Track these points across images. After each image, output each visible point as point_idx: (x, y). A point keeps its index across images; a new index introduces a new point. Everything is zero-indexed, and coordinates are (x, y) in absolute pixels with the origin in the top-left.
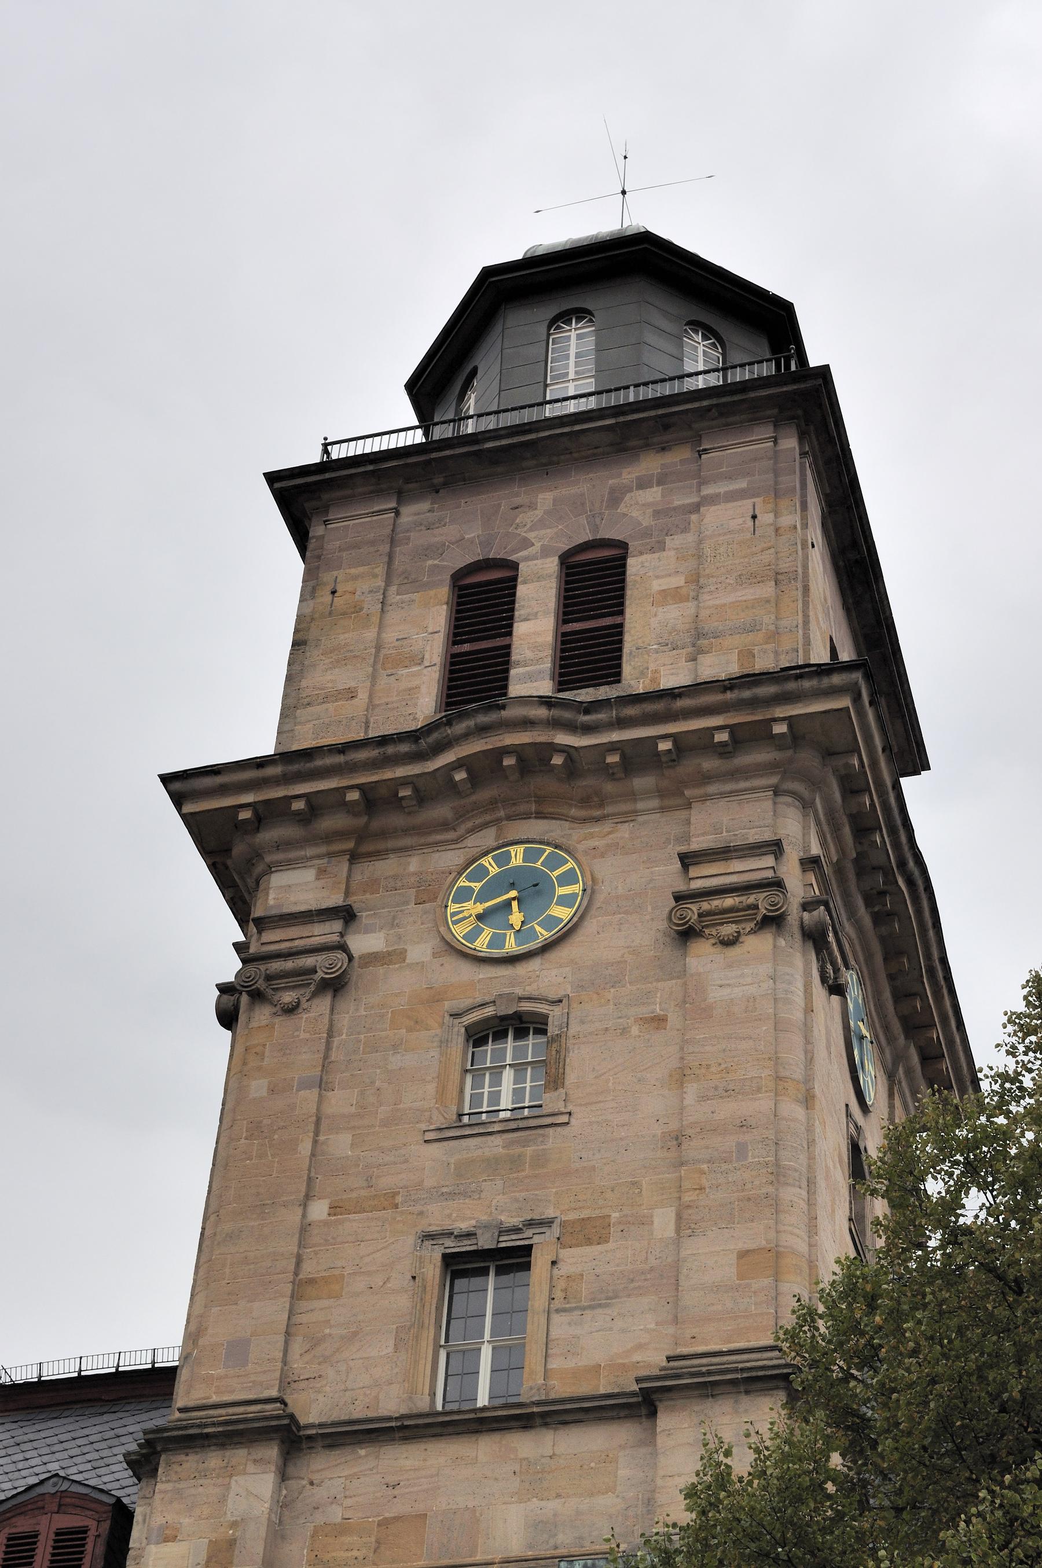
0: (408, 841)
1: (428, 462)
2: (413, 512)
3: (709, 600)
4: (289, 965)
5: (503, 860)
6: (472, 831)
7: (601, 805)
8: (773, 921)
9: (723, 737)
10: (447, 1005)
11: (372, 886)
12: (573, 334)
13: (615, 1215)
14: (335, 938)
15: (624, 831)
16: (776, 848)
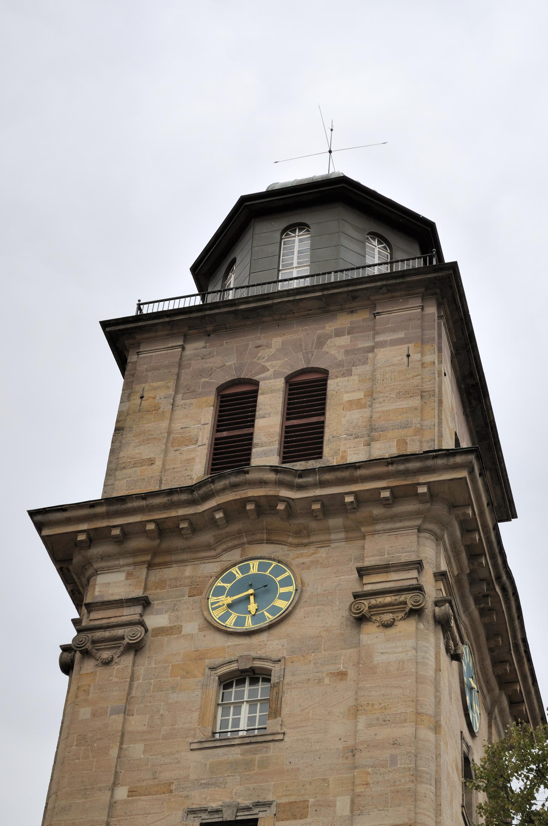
0: (184, 556)
1: (204, 317)
2: (194, 348)
3: (379, 407)
4: (107, 634)
5: (245, 569)
6: (226, 550)
7: (308, 536)
8: (416, 612)
9: (386, 494)
10: (207, 662)
11: (161, 584)
12: (297, 239)
13: (312, 800)
14: (137, 617)
15: (323, 553)
16: (418, 565)
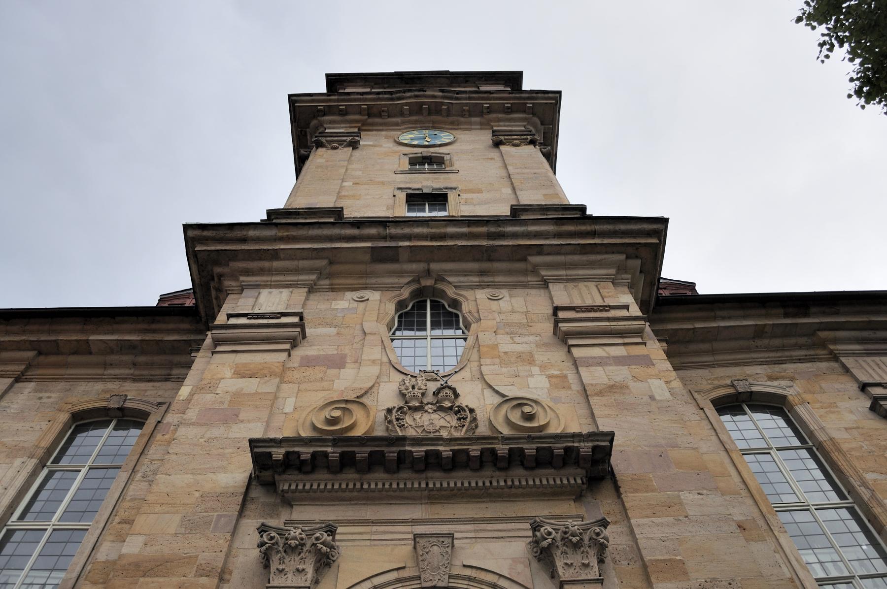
7: (458, 125)
